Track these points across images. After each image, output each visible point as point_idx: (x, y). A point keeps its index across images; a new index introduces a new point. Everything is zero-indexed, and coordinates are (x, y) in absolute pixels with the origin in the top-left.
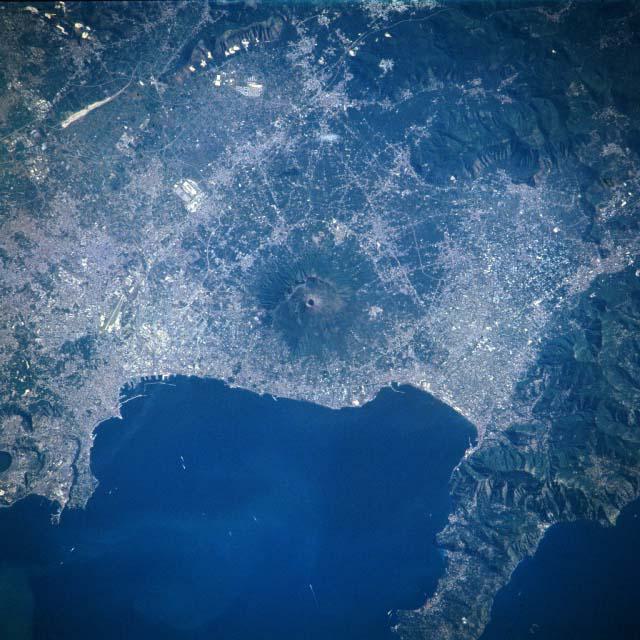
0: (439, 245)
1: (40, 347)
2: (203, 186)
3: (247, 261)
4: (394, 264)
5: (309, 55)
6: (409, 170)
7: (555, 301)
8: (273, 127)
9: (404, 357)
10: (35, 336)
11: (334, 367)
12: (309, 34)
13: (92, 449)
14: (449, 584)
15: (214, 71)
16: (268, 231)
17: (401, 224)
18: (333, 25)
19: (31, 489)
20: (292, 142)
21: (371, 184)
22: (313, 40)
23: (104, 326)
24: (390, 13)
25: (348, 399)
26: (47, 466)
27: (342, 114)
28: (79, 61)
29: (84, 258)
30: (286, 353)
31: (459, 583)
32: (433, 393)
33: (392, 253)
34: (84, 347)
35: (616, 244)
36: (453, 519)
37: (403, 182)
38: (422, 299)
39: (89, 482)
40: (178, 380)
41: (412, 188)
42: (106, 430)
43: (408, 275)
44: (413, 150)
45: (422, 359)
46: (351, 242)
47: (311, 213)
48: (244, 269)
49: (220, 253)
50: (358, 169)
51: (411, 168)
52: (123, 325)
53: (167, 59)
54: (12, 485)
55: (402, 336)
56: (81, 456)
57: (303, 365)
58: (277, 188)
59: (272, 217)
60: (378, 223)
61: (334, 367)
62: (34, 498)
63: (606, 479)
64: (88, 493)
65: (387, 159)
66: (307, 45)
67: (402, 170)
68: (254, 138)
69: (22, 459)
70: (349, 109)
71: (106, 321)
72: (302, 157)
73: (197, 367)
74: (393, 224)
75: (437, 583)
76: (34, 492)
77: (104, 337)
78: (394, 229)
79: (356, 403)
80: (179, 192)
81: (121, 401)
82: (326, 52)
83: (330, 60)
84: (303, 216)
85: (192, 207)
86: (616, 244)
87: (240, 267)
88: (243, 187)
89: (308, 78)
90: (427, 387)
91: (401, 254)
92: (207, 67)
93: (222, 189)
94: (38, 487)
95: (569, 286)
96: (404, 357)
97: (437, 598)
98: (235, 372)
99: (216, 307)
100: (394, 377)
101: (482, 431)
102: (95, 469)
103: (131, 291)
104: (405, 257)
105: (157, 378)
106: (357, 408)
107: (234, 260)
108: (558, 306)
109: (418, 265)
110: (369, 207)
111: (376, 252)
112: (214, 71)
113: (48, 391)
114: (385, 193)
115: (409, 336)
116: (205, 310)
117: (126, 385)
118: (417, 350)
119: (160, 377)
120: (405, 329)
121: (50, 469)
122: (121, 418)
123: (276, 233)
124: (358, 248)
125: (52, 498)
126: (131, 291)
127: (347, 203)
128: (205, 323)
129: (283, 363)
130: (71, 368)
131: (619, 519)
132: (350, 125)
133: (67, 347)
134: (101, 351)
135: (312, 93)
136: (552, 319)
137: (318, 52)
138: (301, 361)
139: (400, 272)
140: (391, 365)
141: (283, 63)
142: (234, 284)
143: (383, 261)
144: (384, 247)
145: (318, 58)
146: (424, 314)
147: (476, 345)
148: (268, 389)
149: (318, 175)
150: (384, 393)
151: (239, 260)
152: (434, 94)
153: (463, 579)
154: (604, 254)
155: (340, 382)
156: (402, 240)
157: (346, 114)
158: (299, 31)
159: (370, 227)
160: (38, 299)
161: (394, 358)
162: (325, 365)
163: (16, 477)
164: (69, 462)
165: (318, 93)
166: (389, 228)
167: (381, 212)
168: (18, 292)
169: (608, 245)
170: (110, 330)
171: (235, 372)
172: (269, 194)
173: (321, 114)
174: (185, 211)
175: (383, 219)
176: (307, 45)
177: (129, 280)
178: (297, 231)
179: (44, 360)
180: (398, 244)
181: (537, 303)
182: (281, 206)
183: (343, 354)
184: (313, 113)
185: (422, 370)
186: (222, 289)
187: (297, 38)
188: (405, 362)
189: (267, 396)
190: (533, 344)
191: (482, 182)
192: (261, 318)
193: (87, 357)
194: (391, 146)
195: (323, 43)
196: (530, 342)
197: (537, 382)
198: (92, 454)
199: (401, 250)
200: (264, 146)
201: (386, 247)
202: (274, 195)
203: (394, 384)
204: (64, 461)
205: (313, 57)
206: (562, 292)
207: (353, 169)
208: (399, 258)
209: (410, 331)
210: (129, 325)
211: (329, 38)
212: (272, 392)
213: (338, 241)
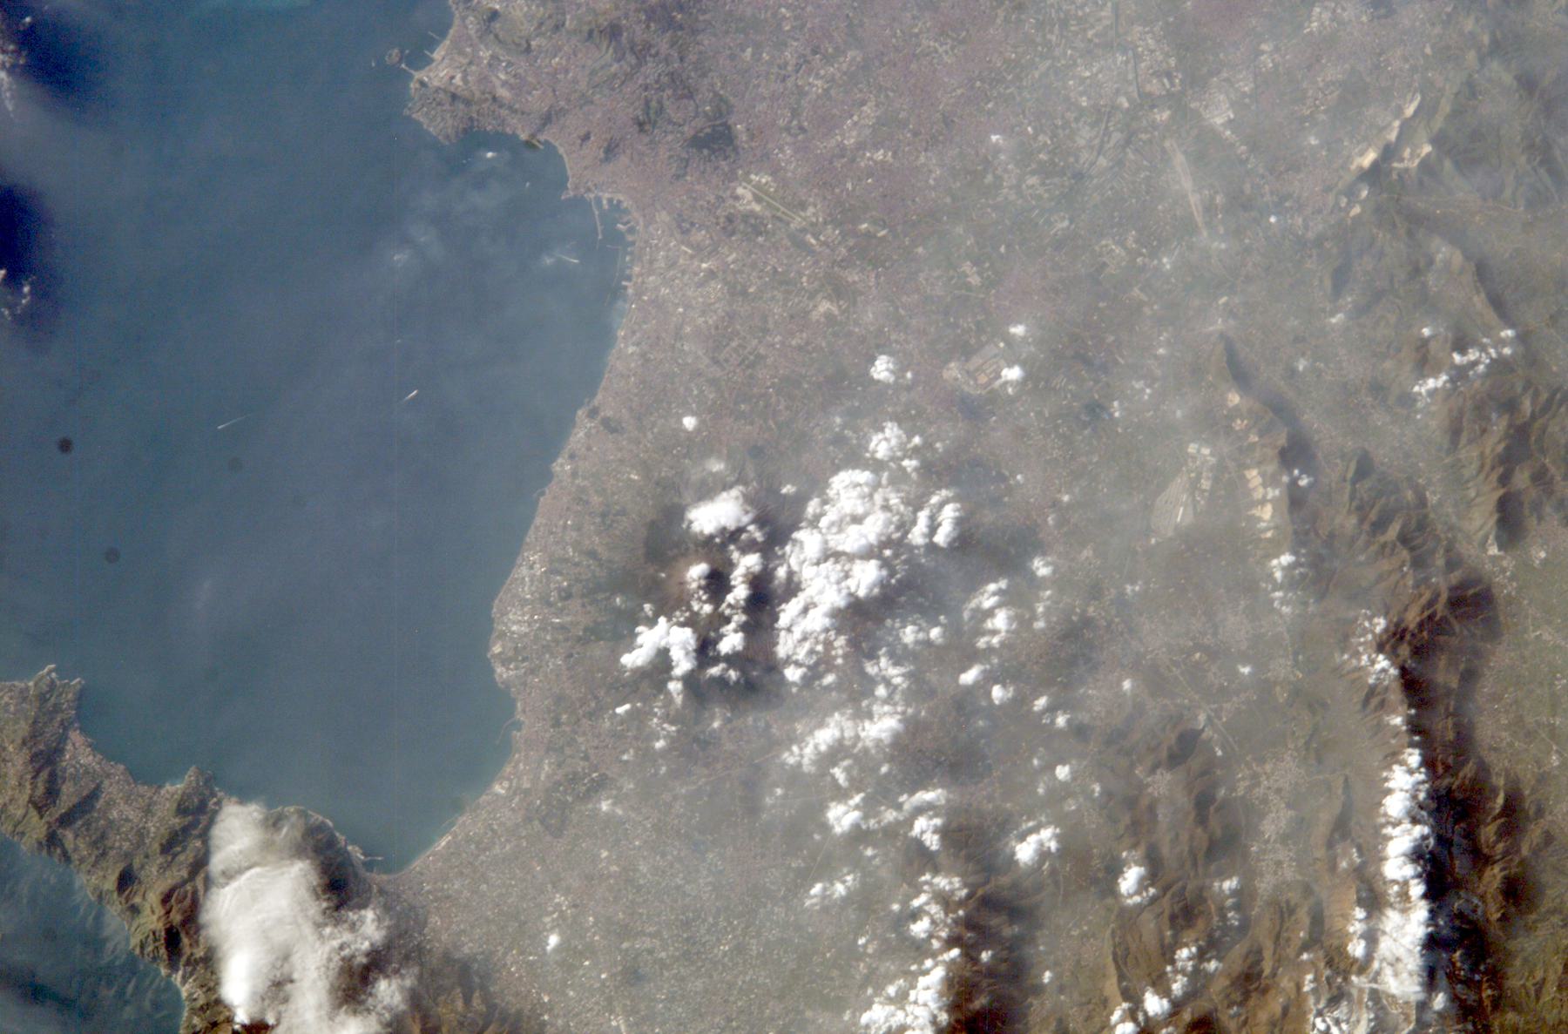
5: (1215, 634)
10: (758, 48)
23: (750, 182)
24: (1265, 801)
29: (895, 154)
32: (484, 798)
57: (592, 554)
71: (758, 186)
73: (631, 350)
76: (457, 21)
77: (731, 177)
79: (497, 649)
81: (598, 200)
98: (606, 422)
105: (628, 272)
106: (487, 648)
113: (641, 61)
119: (629, 278)
125: (438, 54)
138: (600, 550)
140: (557, 723)
153: (114, 814)
162: (583, 596)
170: (740, 191)
193: (698, 142)
204: (504, 84)
205: (1208, 640)
212: (551, 490)
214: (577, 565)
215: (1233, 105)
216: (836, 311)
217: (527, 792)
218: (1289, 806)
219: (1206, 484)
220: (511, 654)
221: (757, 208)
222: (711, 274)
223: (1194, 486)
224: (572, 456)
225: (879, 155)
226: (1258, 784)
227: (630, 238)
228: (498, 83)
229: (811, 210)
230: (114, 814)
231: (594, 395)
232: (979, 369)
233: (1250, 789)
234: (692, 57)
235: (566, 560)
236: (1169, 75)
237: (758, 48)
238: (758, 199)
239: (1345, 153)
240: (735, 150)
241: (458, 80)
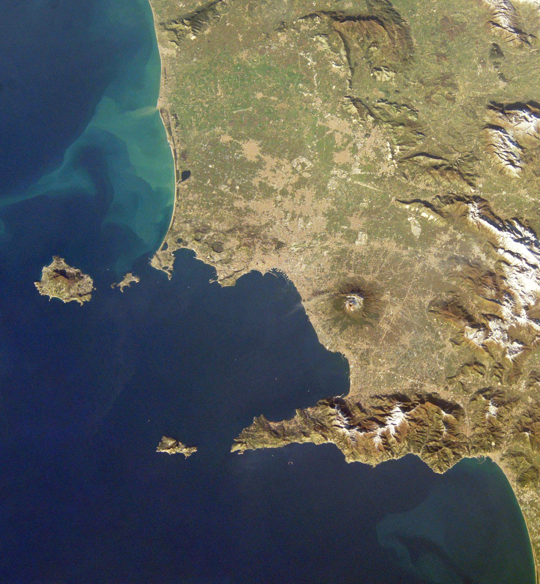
0: (407, 333)
1: (269, 232)
2: (368, 241)
3: (351, 275)
4: (388, 324)
5: (443, 241)
6: (427, 303)
7: (416, 386)
8: (408, 248)
9: (357, 351)
10: (271, 227)
11: (335, 330)
12: (450, 236)
13: (245, 274)
14: (285, 423)
15: (413, 215)
17: (405, 315)
18: (460, 241)
19: (216, 265)
20: (407, 258)
21: (412, 295)
22: (450, 238)
24: (478, 256)
25: (326, 345)
26: (228, 264)
27: (430, 267)
28: (381, 171)
29: (312, 222)
30: (328, 311)
31: (288, 427)
32: (351, 370)
33: (391, 320)
34: (280, 245)
35: (452, 391)
36: (309, 409)
38: (383, 342)
39: (231, 282)
40: (291, 283)
41: (421, 308)
42: (255, 273)
43: (388, 331)
44: (435, 299)
45: (361, 357)
46: (385, 303)
47: (386, 283)
48: (348, 276)
49: (348, 264)
50: (414, 287)
51: (428, 304)
52: (297, 251)
53: (404, 198)
54: (213, 259)
55: (362, 345)
56: (239, 273)
57: (328, 320)
58: (387, 265)
59: (374, 272)
60: (399, 307)
61: (335, 330)
62: (214, 269)
63: (363, 448)
64: (228, 284)
65: (424, 293)
66: (446, 238)
67: (425, 301)
68: (399, 245)
69: (224, 255)
70: (433, 268)
71: (294, 246)
72: (405, 264)
74: (403, 313)
75: (282, 421)
78: (401, 314)
79: (327, 348)
80: (359, 235)
81: (269, 271)
82: (449, 246)
83: (446, 249)
84: (382, 281)
85: (357, 243)
86: (452, 391)
87: (347, 274)
88: (378, 254)
89: (434, 246)
90: (351, 367)
91: (394, 323)
92: (412, 212)
93: (371, 248)
94: (218, 267)
95: (425, 386)
96: (357, 351)
97: (277, 425)
99: (327, 277)
100: (347, 353)
101: (349, 395)
102: (239, 281)
103: (311, 245)
104: (394, 325)
106: (326, 349)
107: (349, 270)
108: (415, 388)
109: (394, 332)
110: (403, 300)
111: (388, 314)
112: (413, 215)
114: (412, 302)
115: (365, 347)
116: (323, 274)
117: (276, 269)
118: (362, 354)
119: (288, 277)
120: (367, 344)
121: (228, 266)
122: (263, 275)
123: (370, 276)
124: (385, 308)
125: (218, 274)
126: (311, 245)
127: (399, 292)
128: (317, 278)
129: (323, 313)
131: (352, 463)
132: (428, 272)
133: (275, 240)
135: (430, 252)
136: (409, 389)
137: (446, 244)
138: (328, 318)
140: (350, 349)
142: (340, 277)
143: (386, 319)
144: (392, 315)
145: (444, 244)
146: (377, 346)
147: (380, 371)
148: (310, 315)
149: (402, 275)
150: (338, 355)
151: (349, 272)
152: (461, 291)
153: (291, 428)
155: (331, 336)
156: (400, 320)
157: (431, 269)
158: (449, 232)
159: (396, 306)
160: (285, 218)
161: (353, 348)
163: (217, 257)
164: (236, 270)
165: (432, 254)
166: (400, 312)
167: (404, 305)
168: (283, 211)
169: (450, 388)
170: (292, 249)
171: (308, 300)
172: (382, 264)
173: (424, 260)
174: (354, 242)
175: (402, 308)
177: (315, 242)
178: (376, 283)
179: (265, 237)
180: (397, 319)
181: (411, 380)
182: (381, 271)
183: (341, 330)
184: (423, 257)
185: (356, 360)
186: (335, 274)
187: (445, 233)
189: (307, 316)
190: (395, 390)
191: (440, 330)
192: (334, 293)
193: (276, 249)
194: (431, 291)
196: (395, 388)
197: (381, 401)
198: (243, 276)
199: (395, 321)
200: (399, 251)
201: (393, 316)
202: (383, 266)
203: (344, 355)
205: (443, 243)
207: (413, 285)
208: (392, 323)
209: (368, 347)
210: (298, 254)
211: (454, 243)
212: (310, 318)
213: (382, 299)
214: (327, 324)
215: (359, 168)
216: (328, 252)
217: (357, 363)
218: (483, 253)
219: (417, 222)
220: (331, 346)
221: (298, 249)
222: (301, 265)
223: (415, 224)
224: (308, 310)
225: (309, 224)
226: (474, 255)
227: (281, 271)
228: (233, 270)
229: (307, 241)
230: (291, 428)
231: (301, 298)
232: (361, 239)
233: (474, 257)
234: (262, 237)
235: (325, 325)
236: (344, 173)
237: (271, 227)
238: (297, 247)
239: (385, 159)
240: (285, 244)
241: (226, 275)
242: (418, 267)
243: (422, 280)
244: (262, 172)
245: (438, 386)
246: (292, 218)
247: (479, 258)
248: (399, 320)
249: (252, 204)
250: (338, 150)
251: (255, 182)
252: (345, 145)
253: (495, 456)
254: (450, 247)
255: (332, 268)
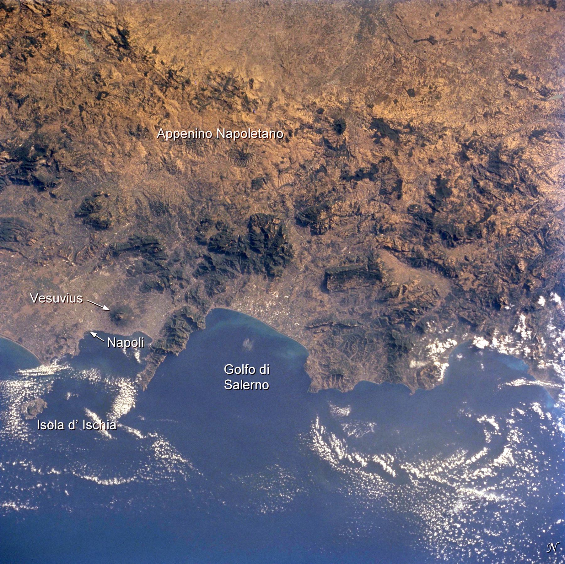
11: (125, 328)
16: (111, 303)
34: (76, 325)
37: (137, 293)
39: (78, 351)
42: (81, 341)
46: (128, 305)
55: (138, 323)
59: (112, 300)
65: (134, 289)
66: (118, 266)
83: (123, 269)
85: (96, 298)
100: (137, 330)
102: (80, 348)
115: (139, 322)
130: (74, 330)
134: (79, 326)
137: (120, 268)
139: (137, 310)
141: (114, 270)
154: (176, 306)
176: (118, 266)
179: (69, 328)
188: (138, 327)
195: (121, 266)
206: (168, 313)
242: (122, 284)
243: (128, 286)
244: (41, 312)
245: (173, 308)
246: (68, 314)
247: (135, 261)
248: (138, 304)
249: (51, 324)
250: (52, 279)
251: (43, 317)
252: (52, 275)
253: (213, 307)
254: (123, 267)
255: (100, 313)
